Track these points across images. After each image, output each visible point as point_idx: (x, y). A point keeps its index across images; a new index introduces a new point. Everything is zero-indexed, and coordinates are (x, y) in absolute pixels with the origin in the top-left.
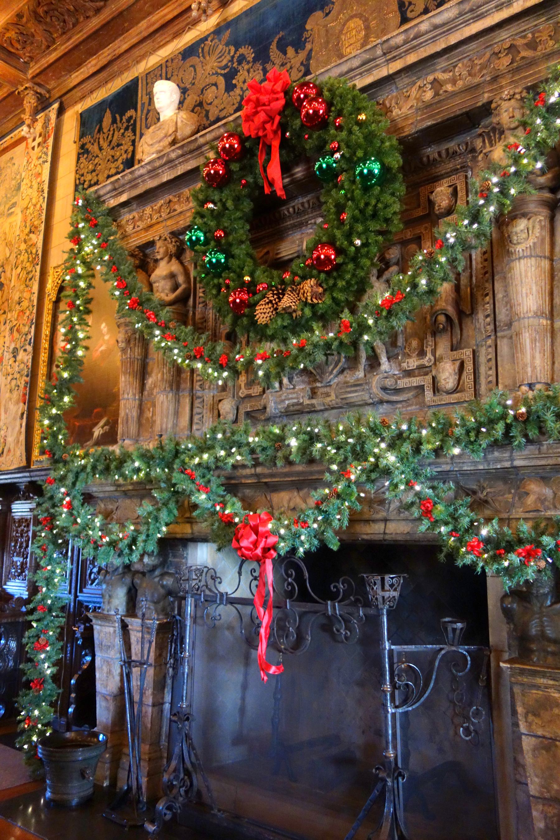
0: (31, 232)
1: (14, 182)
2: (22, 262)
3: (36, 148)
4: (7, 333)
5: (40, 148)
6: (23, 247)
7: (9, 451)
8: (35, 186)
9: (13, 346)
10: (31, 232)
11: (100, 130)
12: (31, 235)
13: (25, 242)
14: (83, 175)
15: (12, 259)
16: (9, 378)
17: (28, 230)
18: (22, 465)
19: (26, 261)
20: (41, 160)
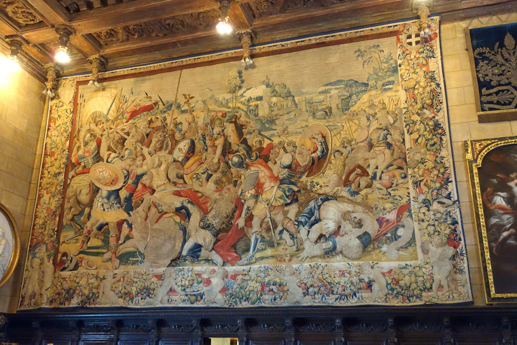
0: (423, 107)
1: (386, 65)
2: (418, 130)
3: (414, 44)
4: (410, 185)
5: (419, 46)
6: (416, 118)
7: (441, 287)
8: (422, 73)
9: (422, 197)
10: (423, 107)
11: (502, 46)
12: (425, 110)
13: (419, 115)
14: (487, 75)
15: (401, 124)
16: (425, 224)
17: (419, 105)
18: (469, 300)
19: (422, 129)
20: (424, 55)
